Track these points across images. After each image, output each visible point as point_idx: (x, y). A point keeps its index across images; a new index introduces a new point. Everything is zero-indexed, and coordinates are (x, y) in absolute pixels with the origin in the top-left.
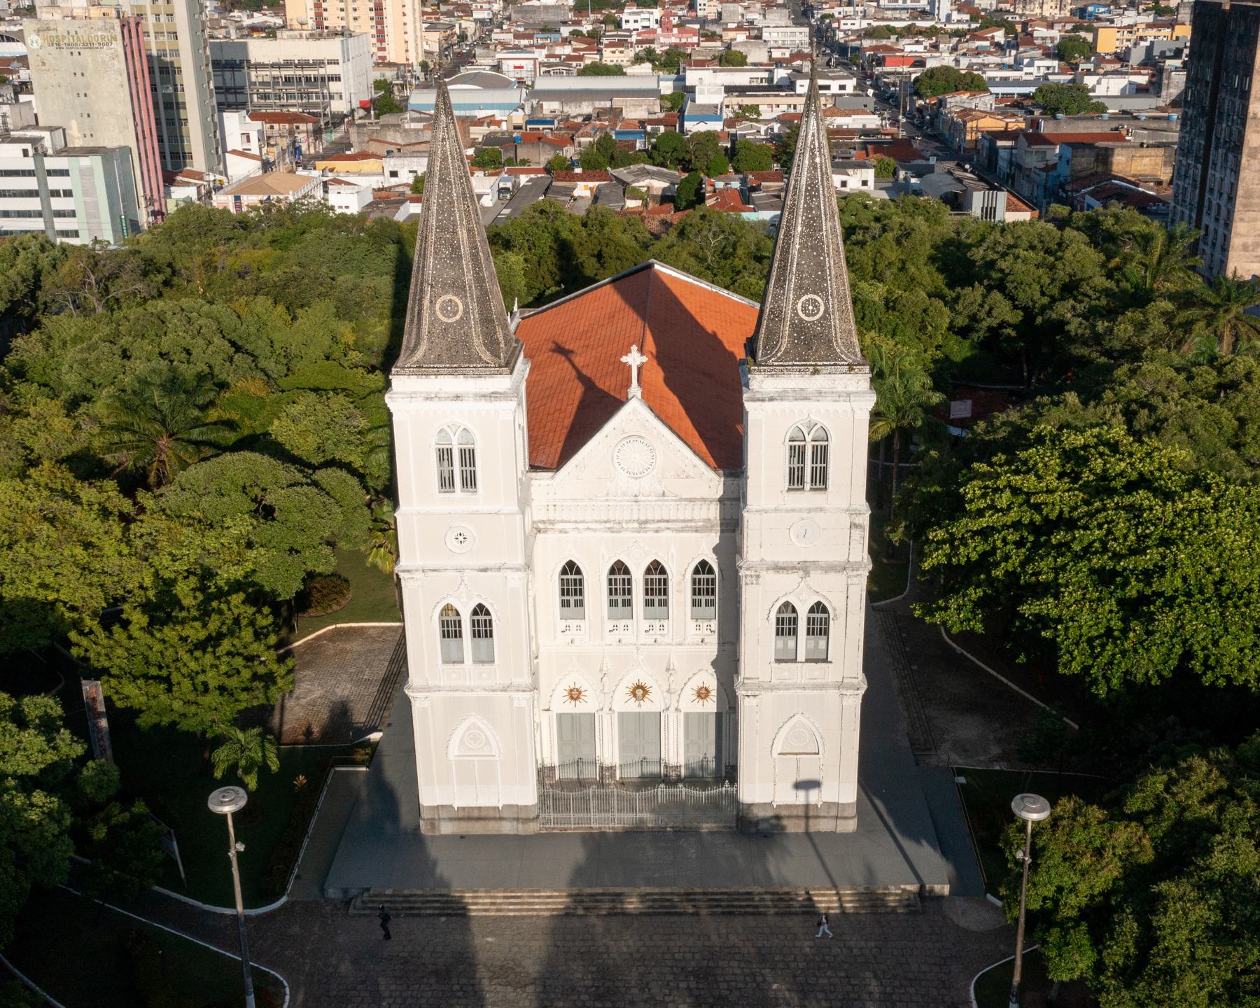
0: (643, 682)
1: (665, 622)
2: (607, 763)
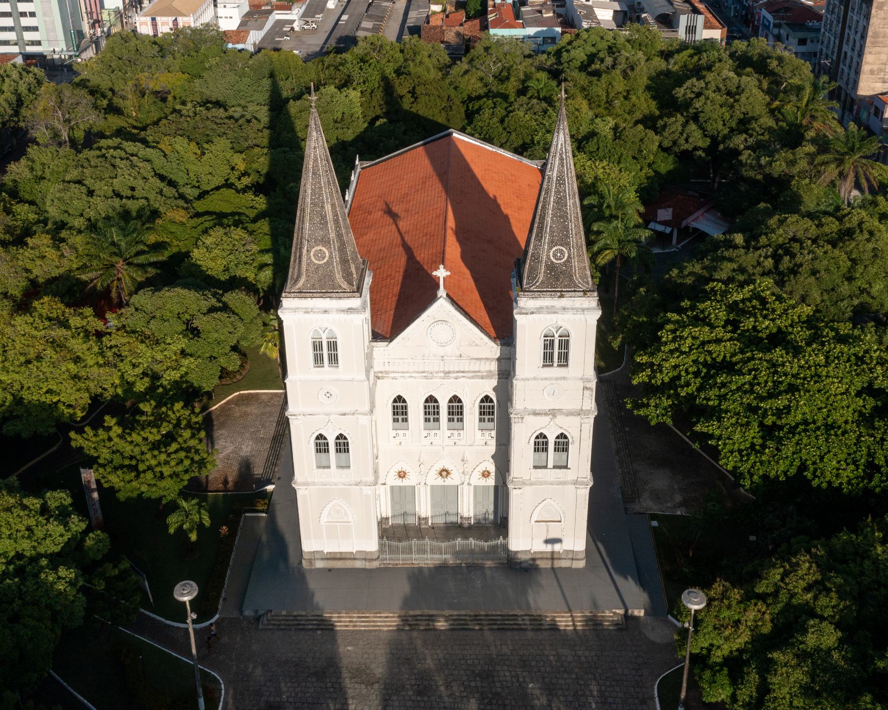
0: (446, 467)
1: (461, 432)
2: (423, 515)
